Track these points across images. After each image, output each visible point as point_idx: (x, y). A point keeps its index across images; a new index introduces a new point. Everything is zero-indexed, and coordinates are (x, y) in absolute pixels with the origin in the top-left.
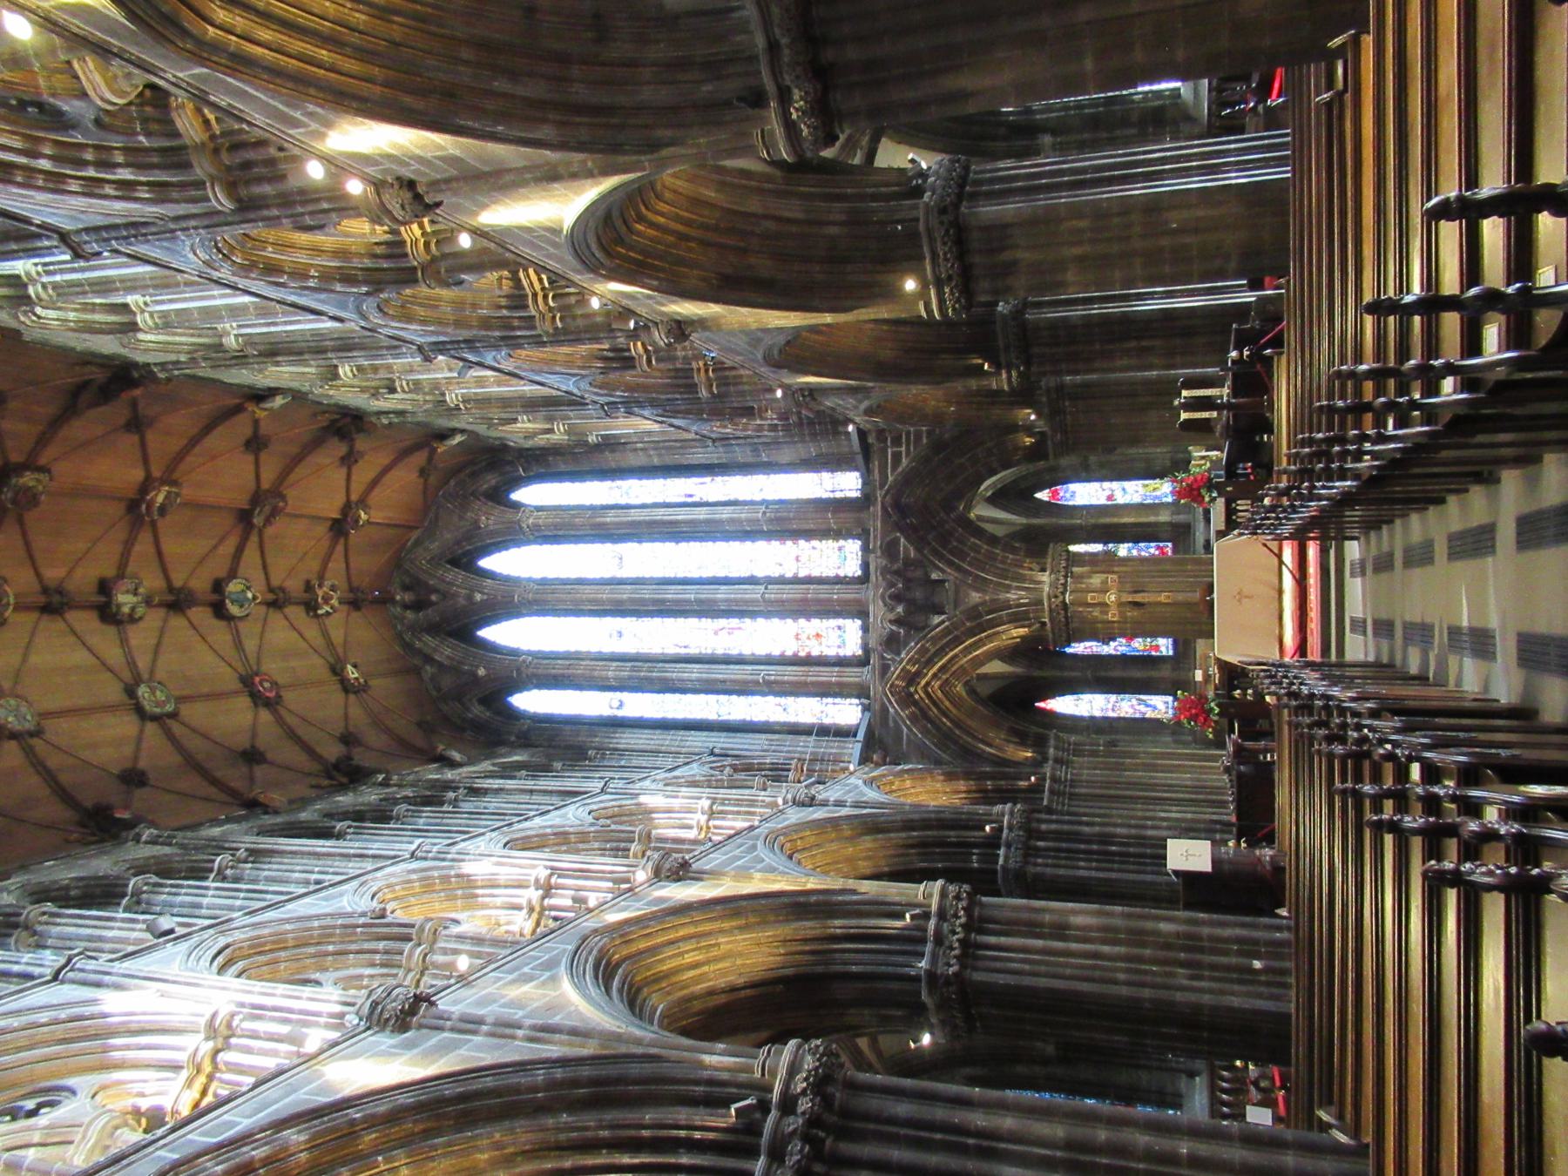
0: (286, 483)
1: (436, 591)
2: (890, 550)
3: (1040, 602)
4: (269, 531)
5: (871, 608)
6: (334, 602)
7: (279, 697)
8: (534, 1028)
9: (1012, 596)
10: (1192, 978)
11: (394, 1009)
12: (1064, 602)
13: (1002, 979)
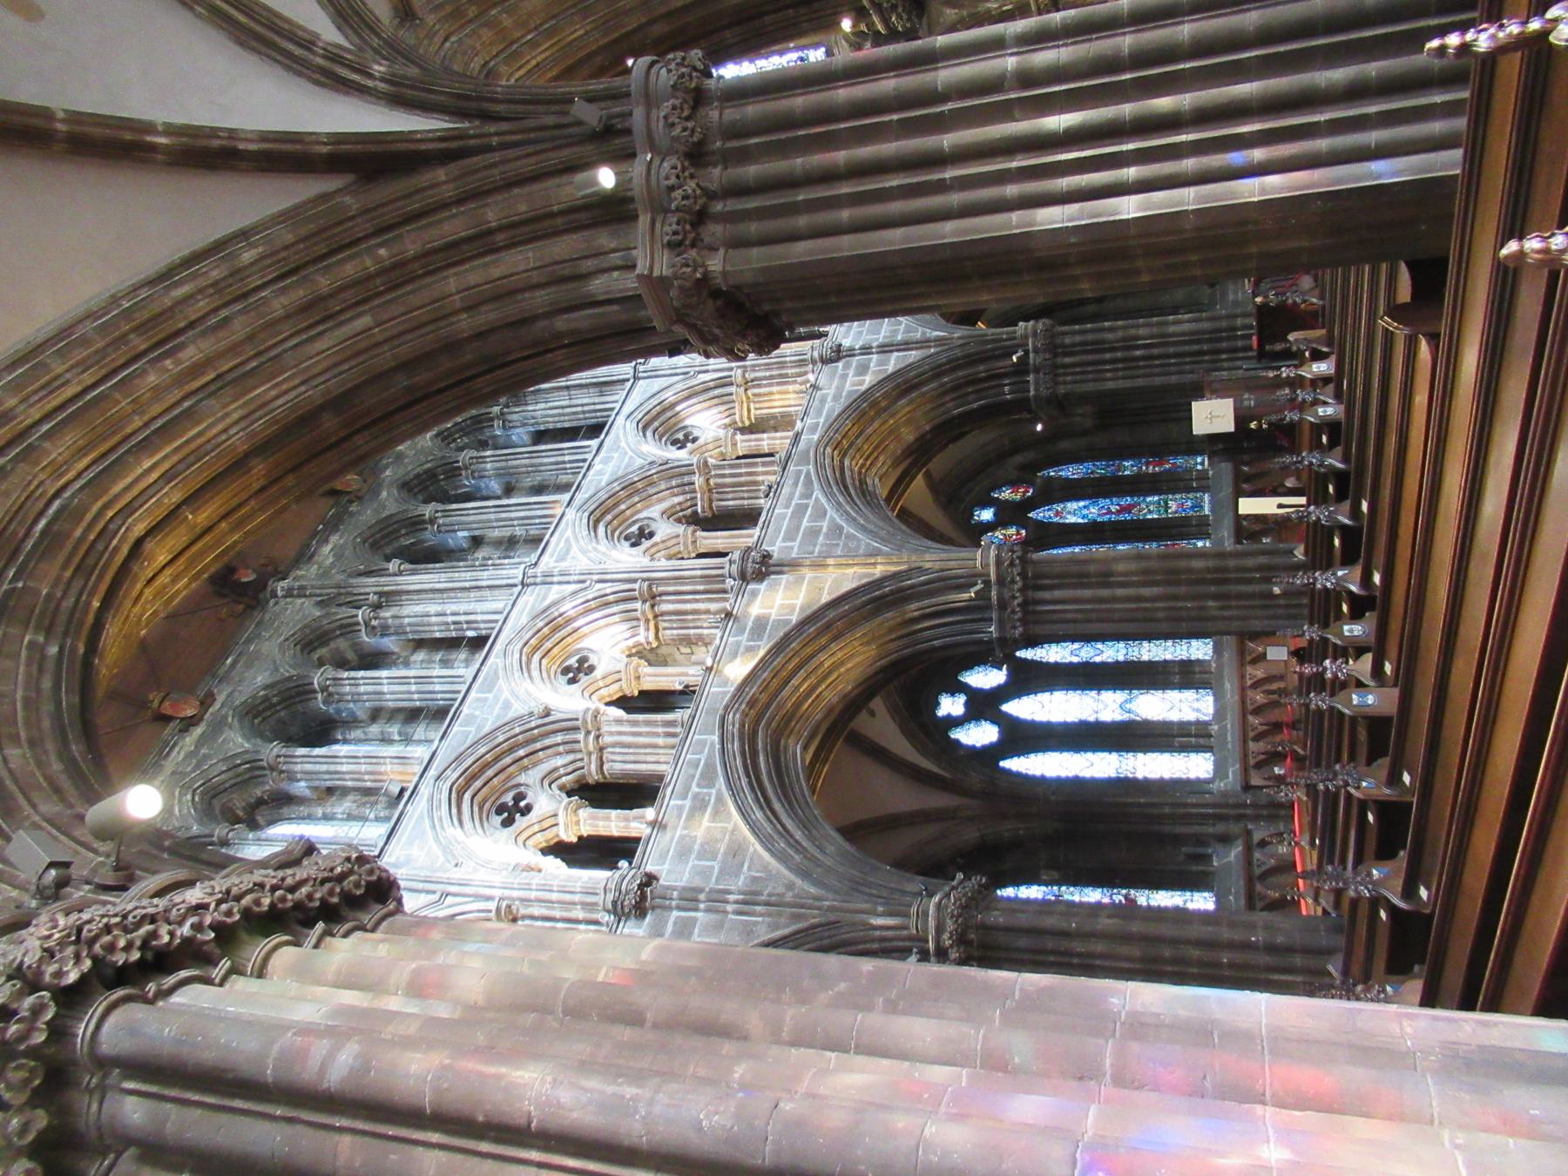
10: (1221, 608)
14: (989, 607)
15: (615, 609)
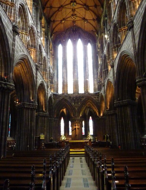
0: (90, 11)
1: (75, 33)
2: (83, 97)
3: (76, 117)
4: (83, 9)
5: (74, 95)
6: (73, 18)
7: (60, 11)
8: (14, 49)
9: (77, 114)
11: (16, 29)
12: (76, 120)
13: (25, 113)
14: (29, 103)
15: (33, 44)
